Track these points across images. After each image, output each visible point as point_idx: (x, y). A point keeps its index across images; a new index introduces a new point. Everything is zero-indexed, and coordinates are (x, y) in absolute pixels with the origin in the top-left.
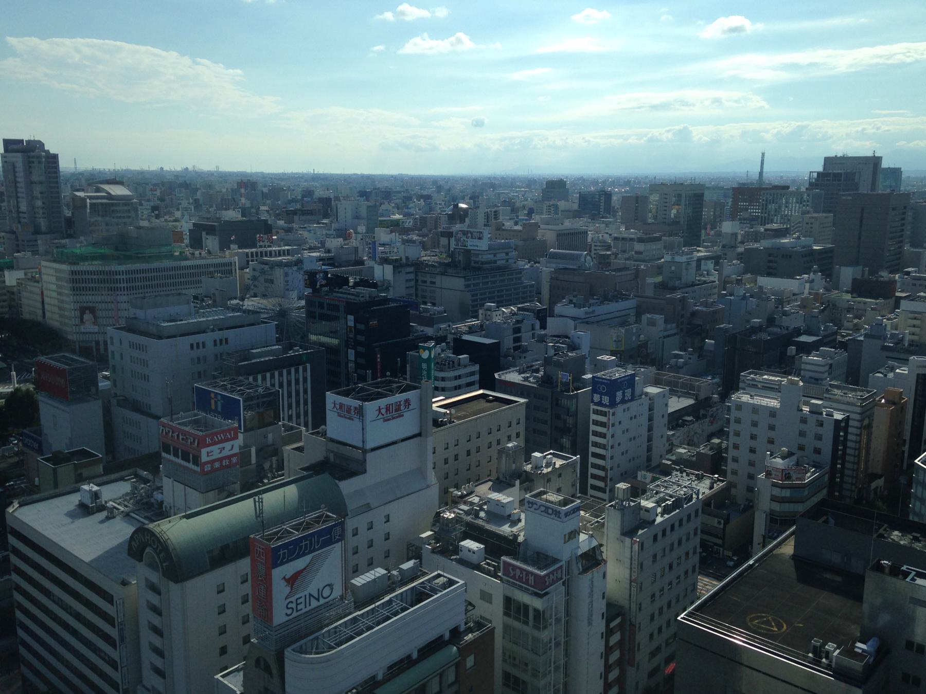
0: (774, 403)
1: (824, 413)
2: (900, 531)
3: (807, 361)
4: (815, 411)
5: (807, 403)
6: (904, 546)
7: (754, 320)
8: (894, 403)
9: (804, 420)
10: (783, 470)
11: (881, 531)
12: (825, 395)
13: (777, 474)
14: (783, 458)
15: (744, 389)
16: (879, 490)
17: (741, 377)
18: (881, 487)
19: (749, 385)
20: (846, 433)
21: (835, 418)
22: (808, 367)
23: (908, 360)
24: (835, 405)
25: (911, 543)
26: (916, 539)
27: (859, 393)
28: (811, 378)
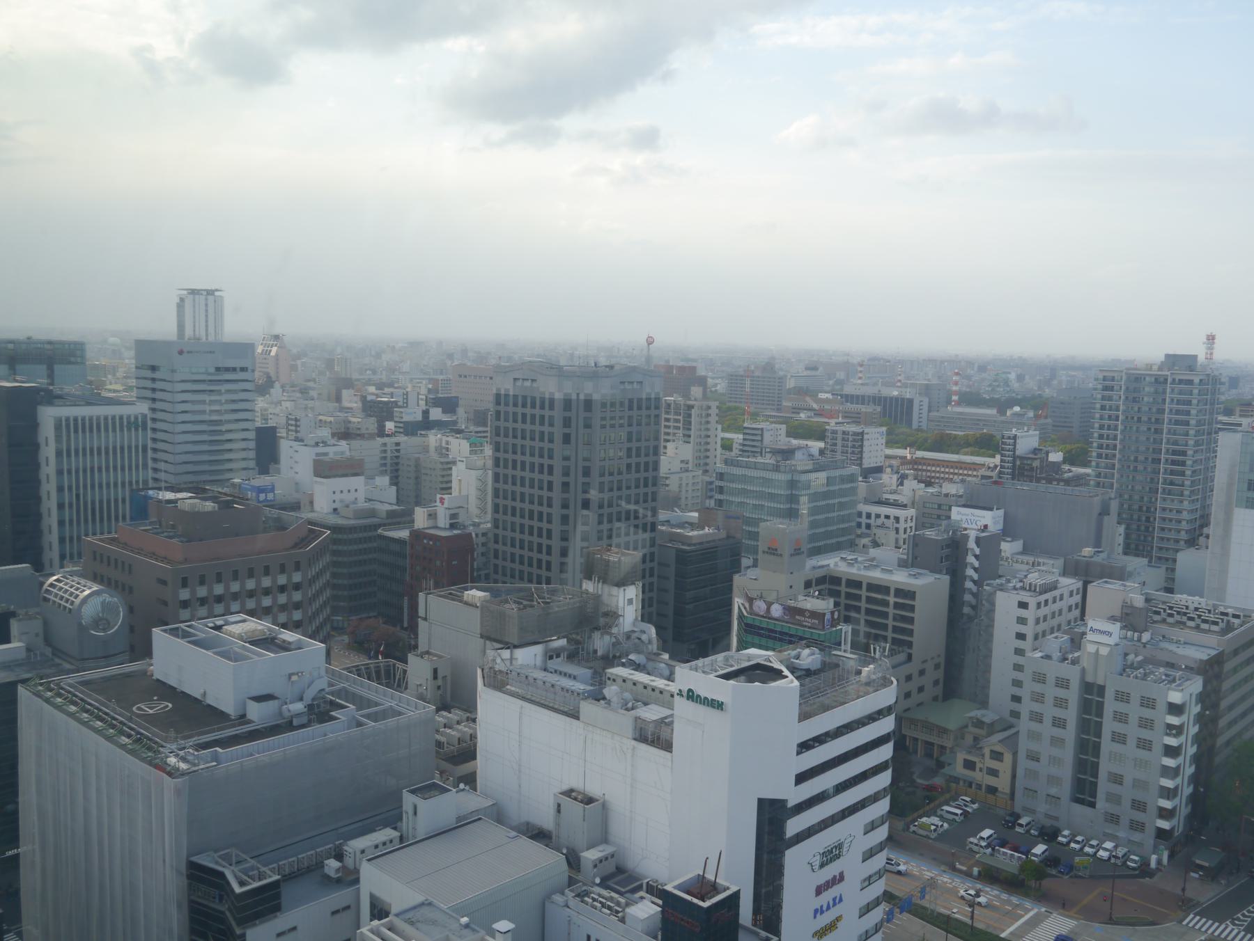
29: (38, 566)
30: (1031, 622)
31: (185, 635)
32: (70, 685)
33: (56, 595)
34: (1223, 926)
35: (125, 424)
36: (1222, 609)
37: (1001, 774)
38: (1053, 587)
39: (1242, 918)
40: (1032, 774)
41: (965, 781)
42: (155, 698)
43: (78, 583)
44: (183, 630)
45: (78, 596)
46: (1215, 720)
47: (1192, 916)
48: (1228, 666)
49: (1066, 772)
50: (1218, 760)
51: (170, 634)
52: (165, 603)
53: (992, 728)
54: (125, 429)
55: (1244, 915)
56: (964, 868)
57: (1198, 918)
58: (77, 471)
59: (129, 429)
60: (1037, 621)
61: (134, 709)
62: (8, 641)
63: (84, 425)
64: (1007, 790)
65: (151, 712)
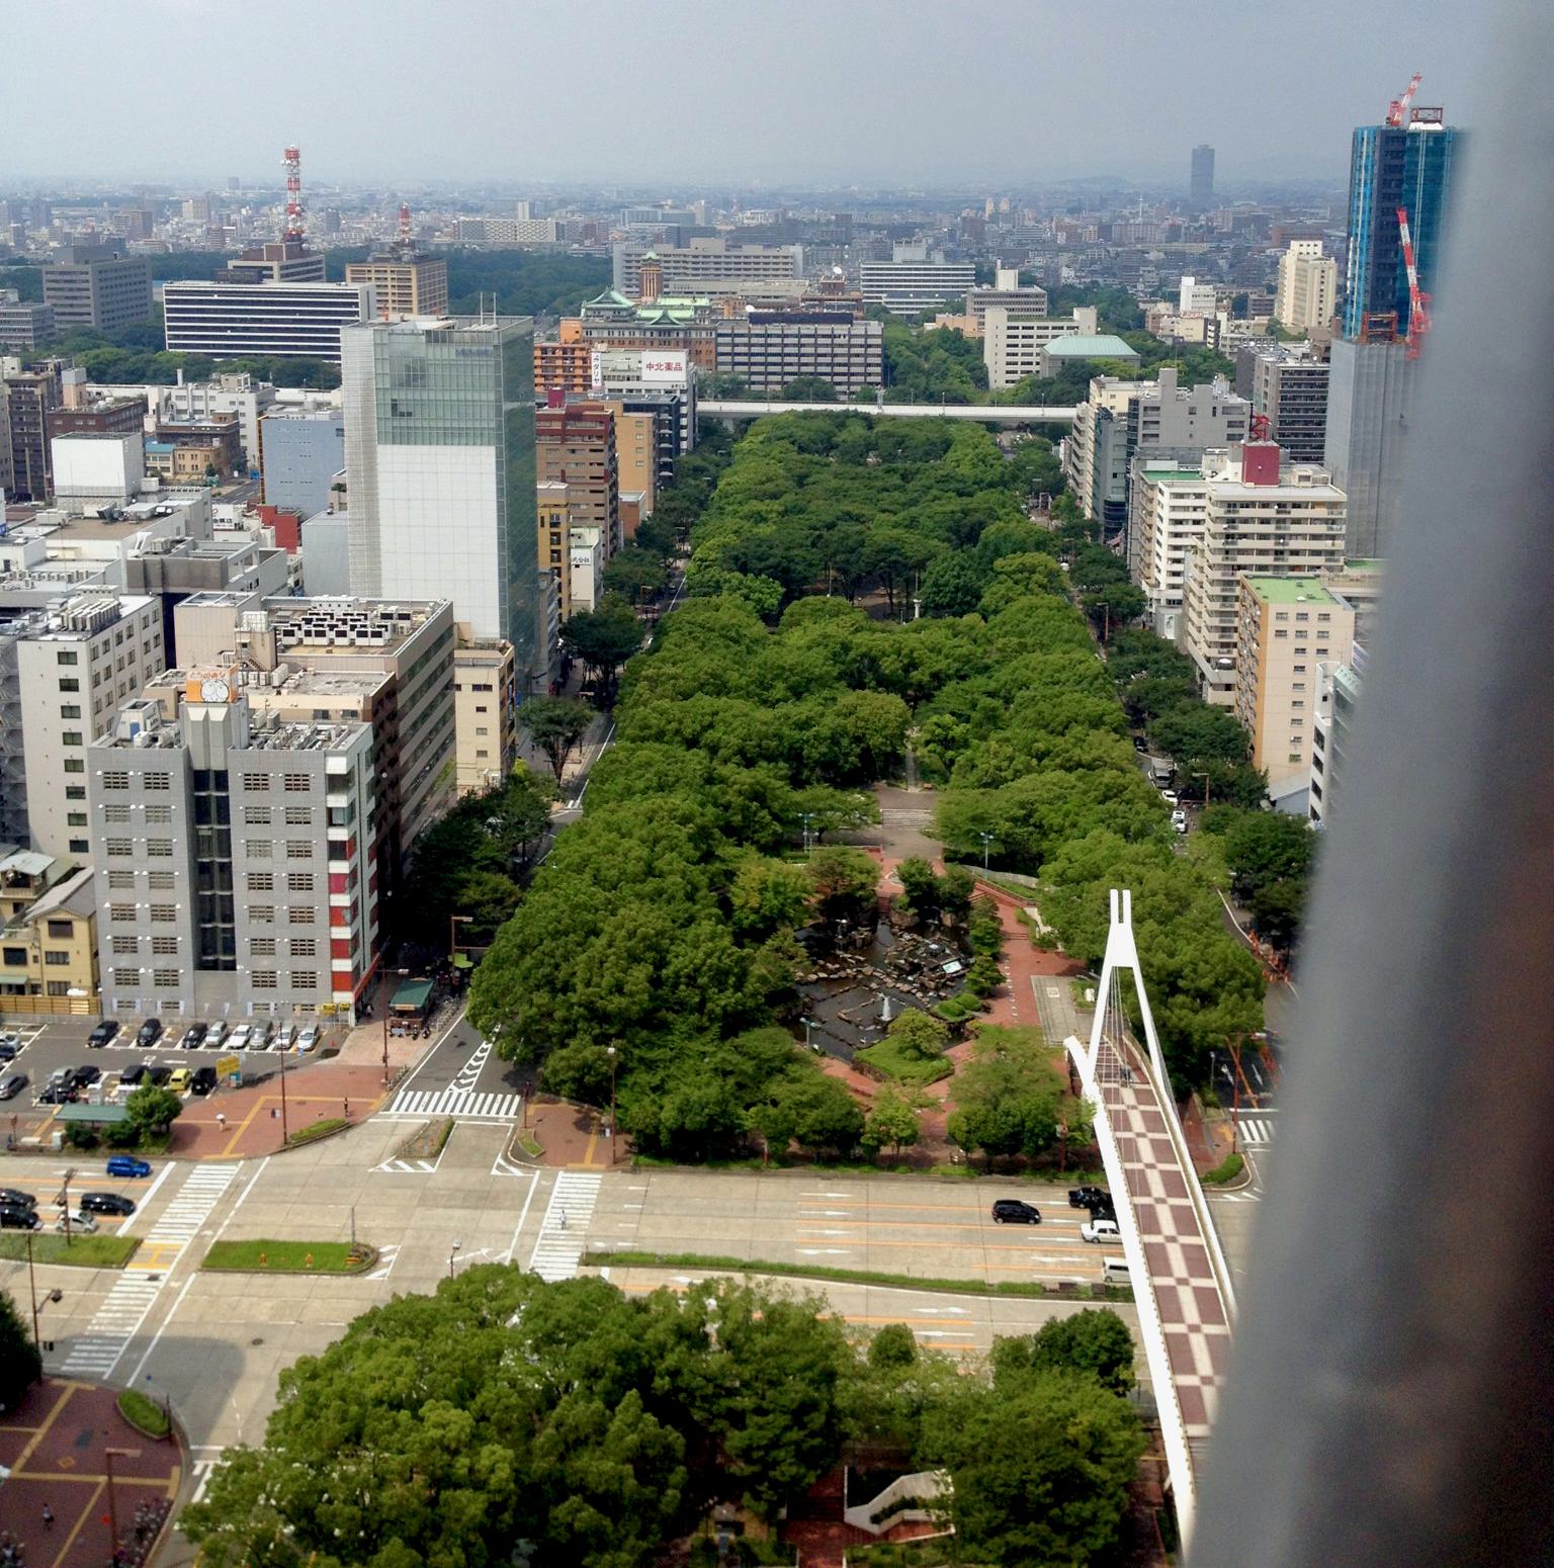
30: (84, 684)
34: (447, 1093)
36: (381, 609)
37: (71, 958)
38: (112, 617)
39: (469, 1072)
40: (125, 945)
41: (10, 987)
46: (394, 783)
47: (402, 1093)
48: (402, 698)
49: (182, 931)
50: (406, 842)
53: (42, 884)
55: (471, 1068)
56: (32, 1140)
57: (411, 1093)
60: (96, 683)
64: (88, 981)
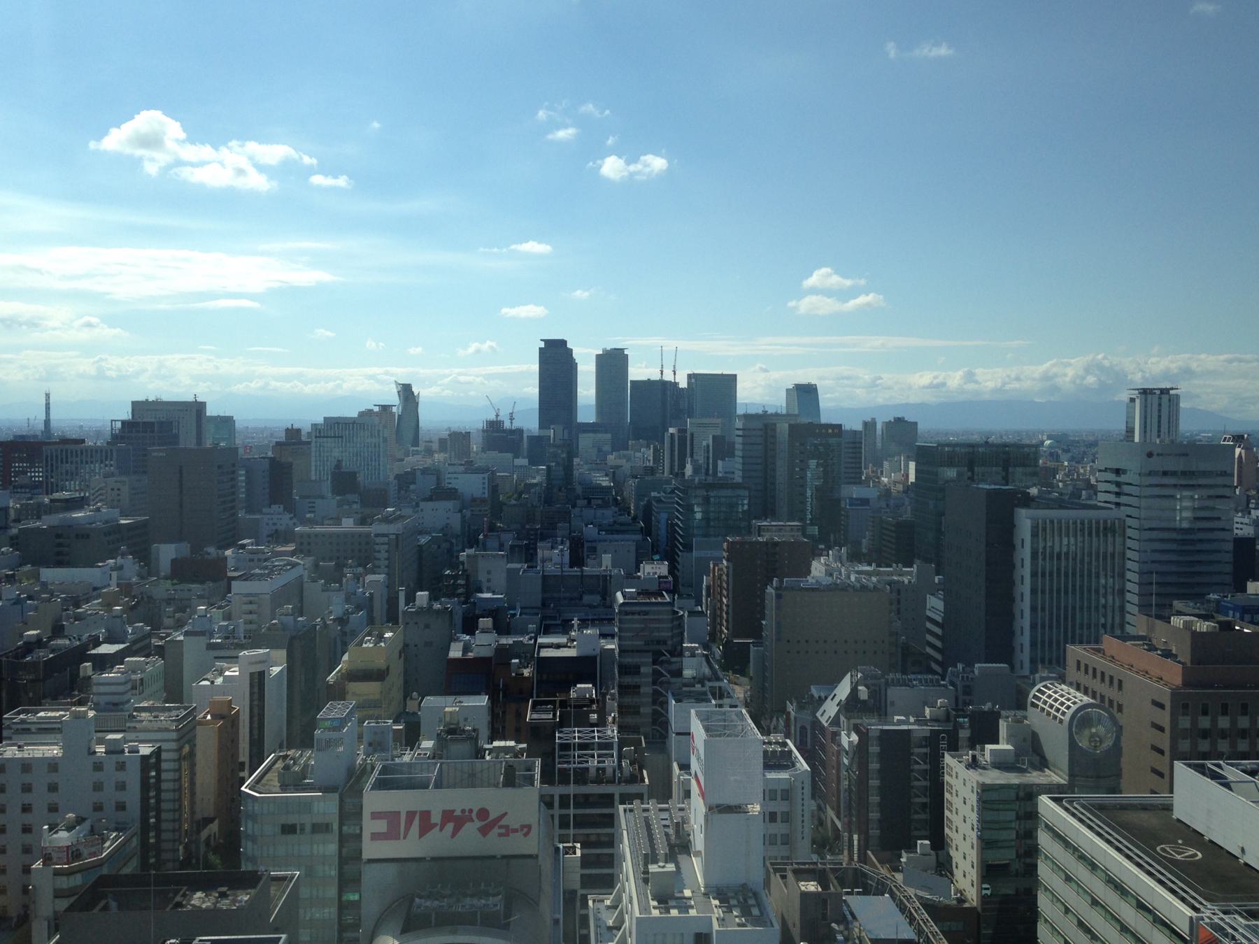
0: (55, 751)
1: (127, 750)
2: (203, 890)
3: (101, 682)
4: (115, 749)
5: (101, 741)
6: (207, 910)
7: (28, 633)
8: (222, 717)
9: (98, 767)
10: (68, 847)
11: (178, 899)
12: (128, 725)
13: (60, 855)
14: (69, 829)
15: (10, 738)
16: (212, 838)
17: (4, 721)
18: (215, 834)
19: (17, 732)
20: (159, 771)
21: (141, 753)
22: (102, 689)
23: (237, 657)
24: (142, 736)
25: (217, 902)
26: (223, 895)
27: (174, 713)
28: (107, 703)
29: (1012, 668)
31: (1215, 776)
32: (1083, 806)
33: (1045, 703)
35: (1102, 529)
42: (1180, 842)
43: (1069, 694)
44: (1209, 768)
45: (1068, 708)
51: (1195, 770)
52: (1161, 729)
54: (1101, 534)
58: (1051, 574)
59: (1105, 535)
61: (1158, 849)
62: (997, 743)
63: (1090, 528)
65: (1179, 857)
